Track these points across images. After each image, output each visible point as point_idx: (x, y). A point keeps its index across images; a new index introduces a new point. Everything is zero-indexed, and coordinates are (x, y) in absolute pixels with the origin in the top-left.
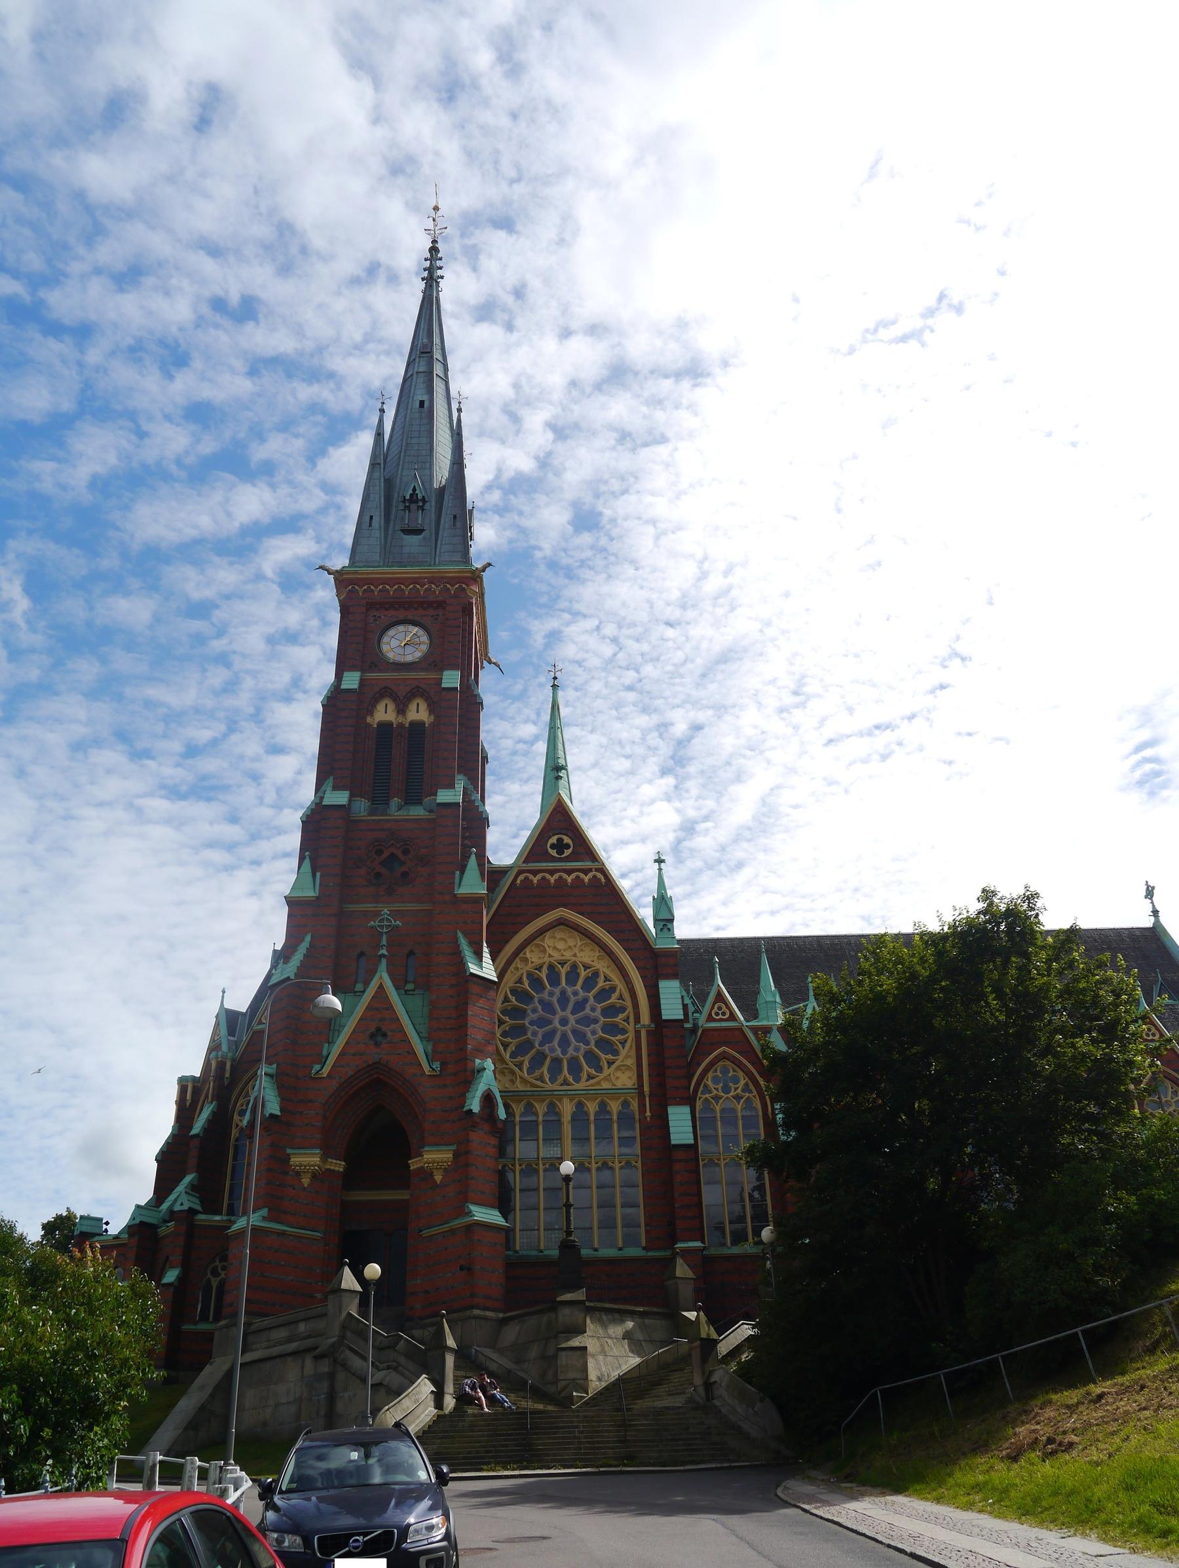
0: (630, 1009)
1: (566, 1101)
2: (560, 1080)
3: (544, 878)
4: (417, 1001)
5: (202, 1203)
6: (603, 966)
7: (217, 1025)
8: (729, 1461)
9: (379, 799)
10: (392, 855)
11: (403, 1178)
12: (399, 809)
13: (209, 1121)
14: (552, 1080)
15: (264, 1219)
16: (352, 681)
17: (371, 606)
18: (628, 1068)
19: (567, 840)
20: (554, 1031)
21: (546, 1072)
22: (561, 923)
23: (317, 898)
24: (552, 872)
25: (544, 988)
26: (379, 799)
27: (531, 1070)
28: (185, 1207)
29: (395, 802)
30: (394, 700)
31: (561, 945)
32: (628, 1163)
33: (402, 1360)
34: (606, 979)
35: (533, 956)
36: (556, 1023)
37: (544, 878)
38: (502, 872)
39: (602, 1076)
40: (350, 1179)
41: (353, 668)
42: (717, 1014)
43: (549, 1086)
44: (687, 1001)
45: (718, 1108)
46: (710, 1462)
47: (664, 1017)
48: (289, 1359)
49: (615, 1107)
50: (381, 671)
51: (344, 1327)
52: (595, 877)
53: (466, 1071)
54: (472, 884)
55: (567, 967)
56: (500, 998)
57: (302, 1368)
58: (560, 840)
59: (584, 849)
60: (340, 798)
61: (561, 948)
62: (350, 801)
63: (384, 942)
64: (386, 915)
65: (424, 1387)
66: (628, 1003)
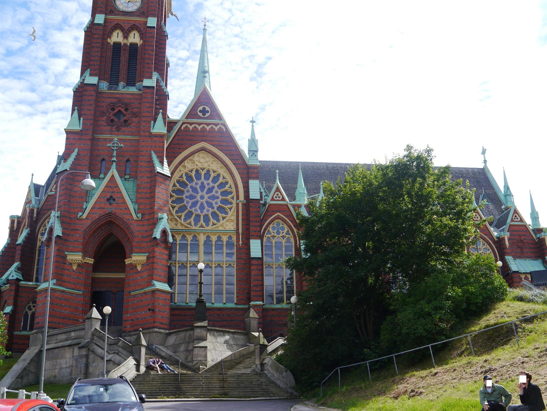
0: (234, 193)
1: (202, 235)
2: (199, 225)
3: (195, 127)
4: (131, 184)
5: (23, 276)
6: (223, 172)
7: (30, 191)
8: (271, 397)
9: (114, 82)
10: (120, 110)
11: (122, 268)
12: (124, 88)
13: (26, 237)
14: (196, 224)
15: (54, 284)
18: (232, 221)
19: (207, 108)
20: (197, 202)
21: (192, 221)
22: (203, 149)
23: (81, 131)
25: (193, 181)
26: (114, 82)
27: (185, 220)
28: (15, 278)
29: (121, 84)
30: (122, 31)
31: (202, 160)
32: (230, 265)
33: (121, 350)
34: (224, 178)
35: (188, 165)
36: (198, 198)
37: (195, 127)
39: (219, 224)
40: (96, 267)
41: (101, 12)
42: (276, 197)
43: (194, 228)
44: (262, 190)
45: (274, 242)
46: (261, 397)
47: (251, 198)
48: (67, 348)
49: (225, 239)
50: (115, 15)
51: (93, 335)
52: (220, 128)
53: (153, 218)
54: (159, 128)
55: (205, 171)
56: (172, 185)
57: (73, 352)
58: (204, 108)
59: (215, 114)
60: (94, 80)
61: (202, 161)
62: (98, 82)
63: (115, 154)
64: (115, 141)
65: (131, 362)
66: (234, 190)
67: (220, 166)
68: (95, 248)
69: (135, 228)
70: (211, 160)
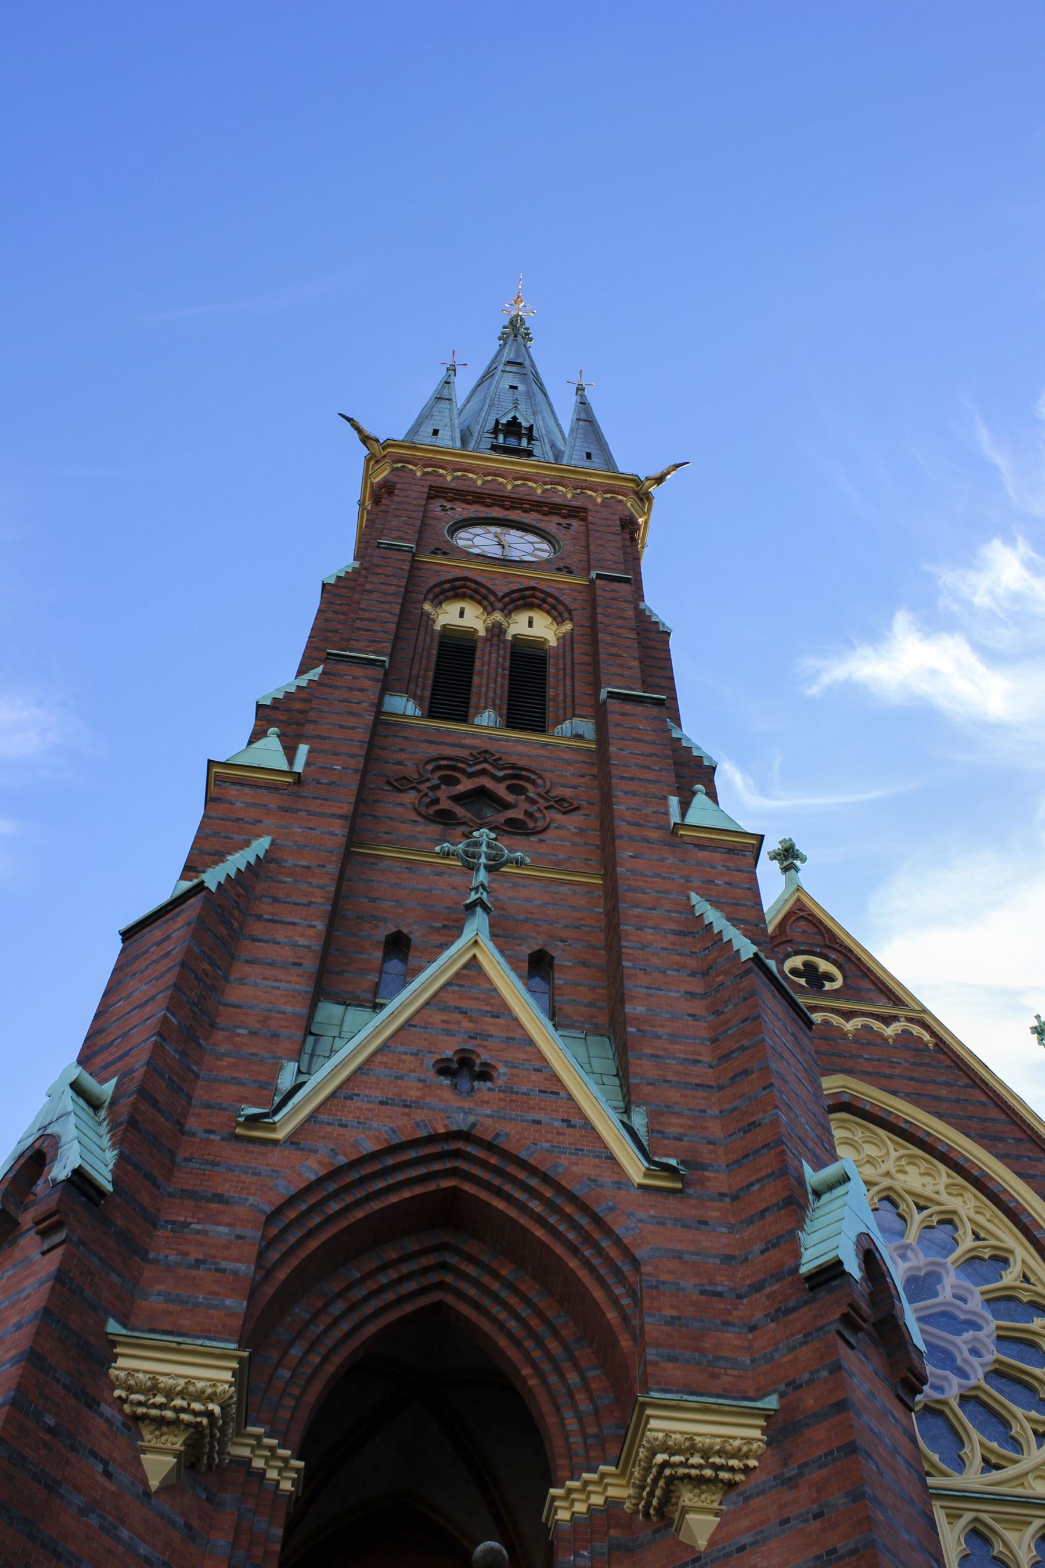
6: (967, 1205)
19: (824, 966)
29: (487, 718)
67: (945, 1180)
68: (317, 1387)
69: (639, 1226)
70: (894, 1155)
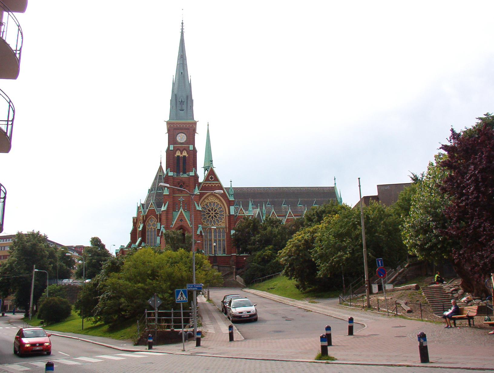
4: (188, 214)
9: (178, 172)
16: (172, 148)
17: (175, 129)
24: (210, 184)
38: (200, 183)
59: (217, 179)
